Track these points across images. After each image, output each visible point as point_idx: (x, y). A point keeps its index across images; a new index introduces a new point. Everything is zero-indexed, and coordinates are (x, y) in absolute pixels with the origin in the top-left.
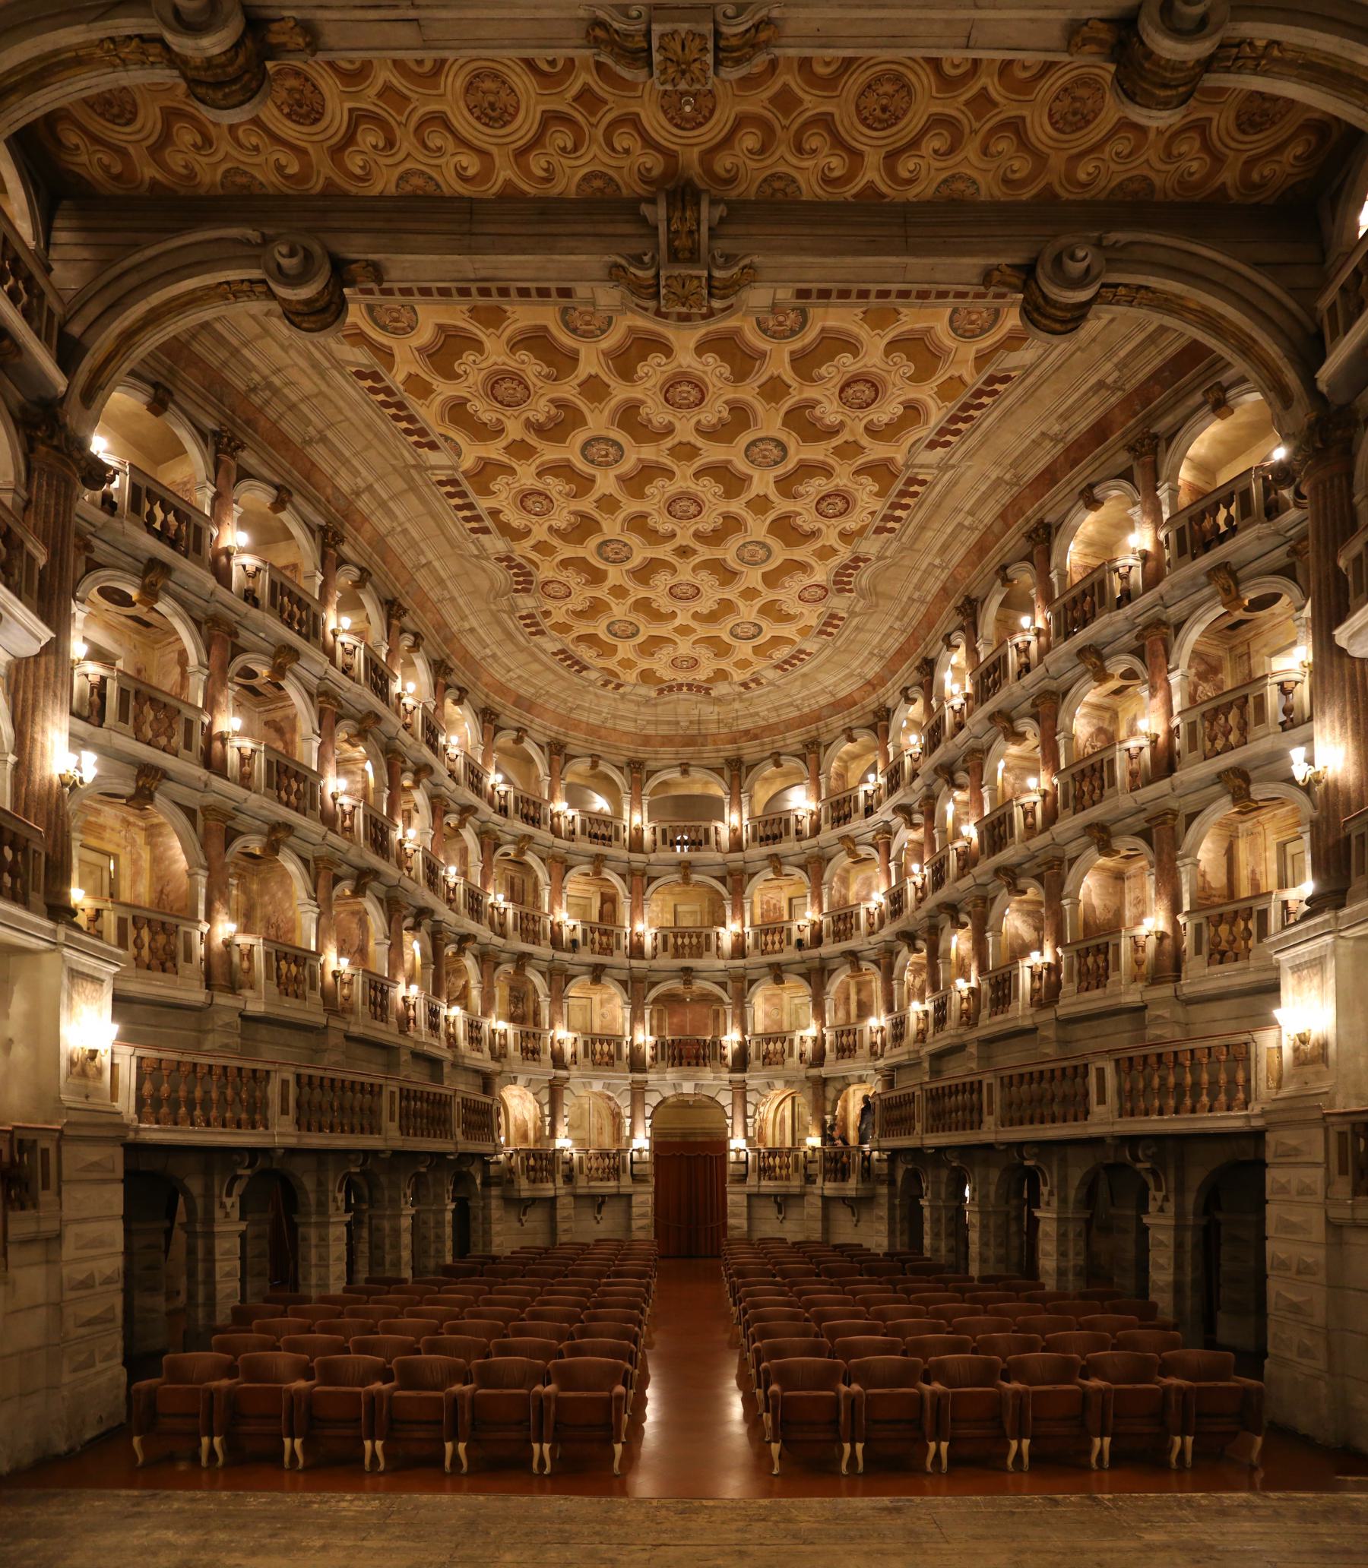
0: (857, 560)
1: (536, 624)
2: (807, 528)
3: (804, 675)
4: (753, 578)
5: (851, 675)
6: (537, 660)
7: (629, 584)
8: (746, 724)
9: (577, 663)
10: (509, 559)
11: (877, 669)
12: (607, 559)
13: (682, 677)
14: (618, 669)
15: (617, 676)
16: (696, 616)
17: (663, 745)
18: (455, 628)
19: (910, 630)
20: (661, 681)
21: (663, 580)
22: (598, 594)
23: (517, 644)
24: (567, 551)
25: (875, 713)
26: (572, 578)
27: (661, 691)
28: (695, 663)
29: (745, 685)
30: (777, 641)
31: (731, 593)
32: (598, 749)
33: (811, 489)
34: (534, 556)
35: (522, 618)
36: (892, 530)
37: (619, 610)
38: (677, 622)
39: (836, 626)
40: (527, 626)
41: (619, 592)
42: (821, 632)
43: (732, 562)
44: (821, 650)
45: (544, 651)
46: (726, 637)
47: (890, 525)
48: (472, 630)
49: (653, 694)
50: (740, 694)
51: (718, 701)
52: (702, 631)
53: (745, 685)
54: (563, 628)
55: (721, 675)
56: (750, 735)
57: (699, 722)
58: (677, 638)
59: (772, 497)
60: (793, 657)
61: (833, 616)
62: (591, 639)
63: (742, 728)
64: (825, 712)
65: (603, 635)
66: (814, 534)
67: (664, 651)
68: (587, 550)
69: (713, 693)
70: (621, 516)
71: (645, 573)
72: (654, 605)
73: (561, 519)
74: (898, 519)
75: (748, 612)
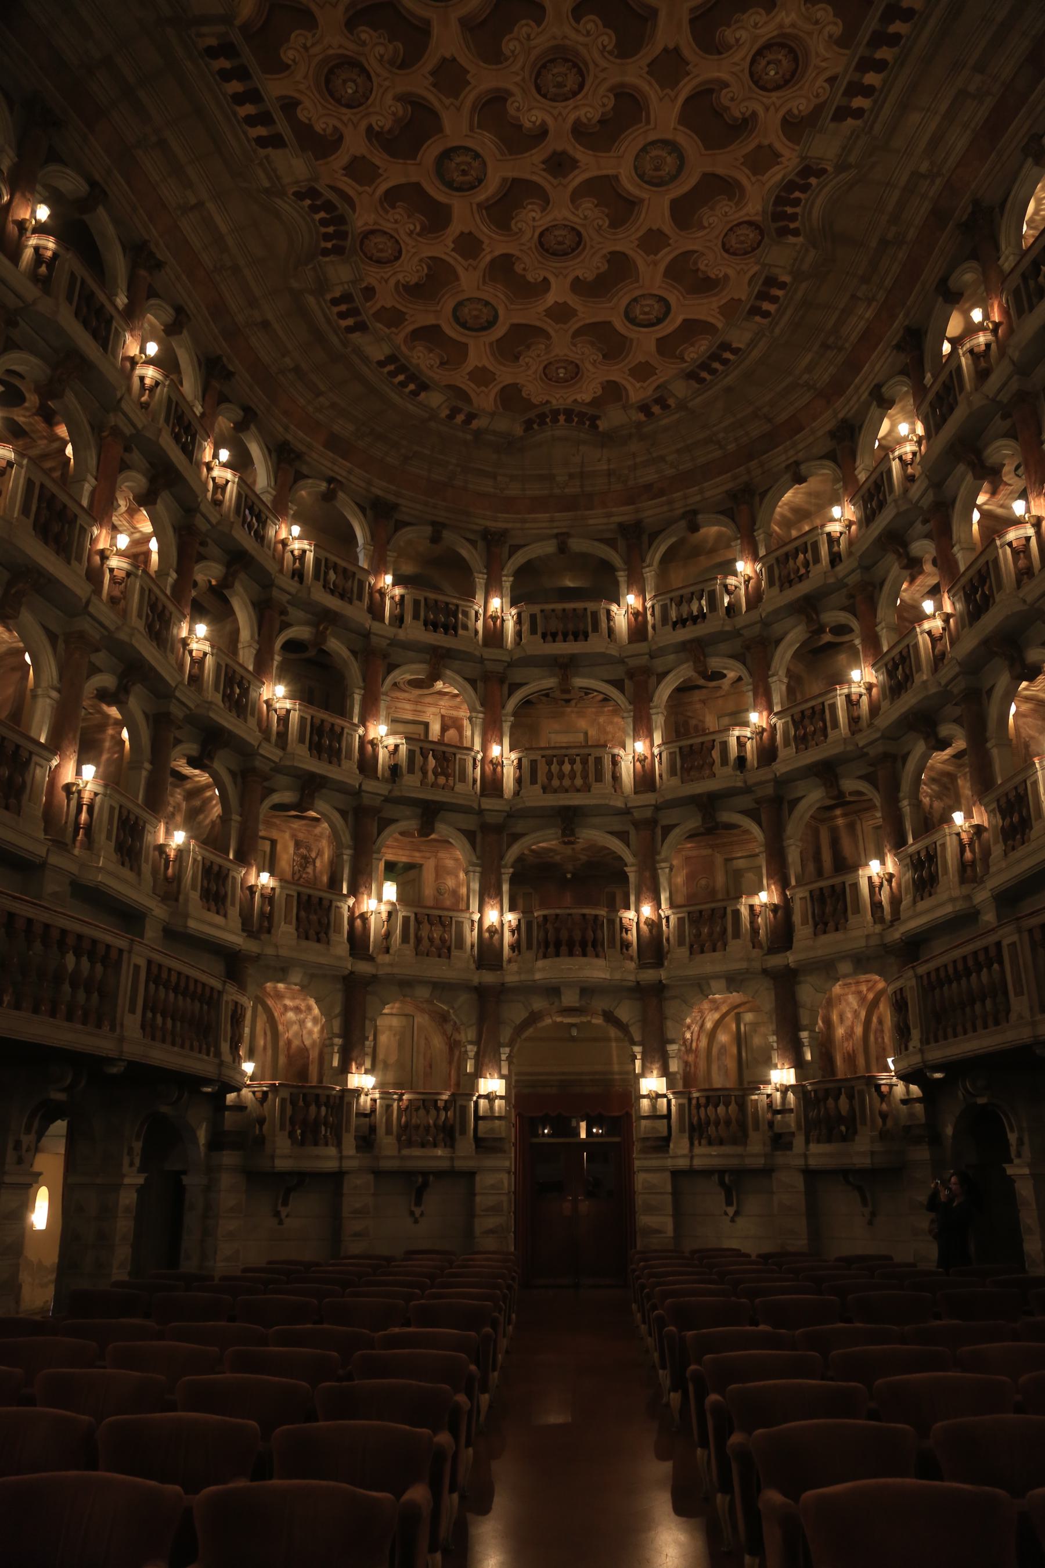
0: (807, 171)
1: (354, 312)
2: (737, 111)
4: (656, 210)
7: (485, 232)
9: (412, 378)
10: (312, 193)
12: (450, 185)
13: (560, 398)
14: (469, 387)
15: (465, 397)
16: (578, 286)
21: (531, 219)
22: (437, 251)
24: (395, 174)
25: (832, 434)
26: (401, 223)
27: (528, 425)
28: (575, 373)
30: (692, 328)
31: (626, 242)
33: (743, 35)
34: (347, 185)
35: (335, 302)
36: (859, 113)
37: (469, 281)
38: (551, 298)
39: (774, 300)
40: (342, 315)
41: (468, 246)
42: (755, 311)
43: (630, 185)
46: (620, 325)
47: (858, 102)
48: (265, 325)
49: (518, 430)
52: (587, 313)
53: (644, 408)
54: (394, 318)
55: (613, 391)
58: (550, 326)
59: (687, 53)
60: (714, 357)
61: (771, 281)
62: (430, 335)
65: (451, 331)
66: (745, 125)
68: (419, 171)
69: (602, 425)
70: (469, 97)
71: (502, 210)
72: (518, 268)
73: (385, 111)
74: (868, 91)
75: (651, 275)
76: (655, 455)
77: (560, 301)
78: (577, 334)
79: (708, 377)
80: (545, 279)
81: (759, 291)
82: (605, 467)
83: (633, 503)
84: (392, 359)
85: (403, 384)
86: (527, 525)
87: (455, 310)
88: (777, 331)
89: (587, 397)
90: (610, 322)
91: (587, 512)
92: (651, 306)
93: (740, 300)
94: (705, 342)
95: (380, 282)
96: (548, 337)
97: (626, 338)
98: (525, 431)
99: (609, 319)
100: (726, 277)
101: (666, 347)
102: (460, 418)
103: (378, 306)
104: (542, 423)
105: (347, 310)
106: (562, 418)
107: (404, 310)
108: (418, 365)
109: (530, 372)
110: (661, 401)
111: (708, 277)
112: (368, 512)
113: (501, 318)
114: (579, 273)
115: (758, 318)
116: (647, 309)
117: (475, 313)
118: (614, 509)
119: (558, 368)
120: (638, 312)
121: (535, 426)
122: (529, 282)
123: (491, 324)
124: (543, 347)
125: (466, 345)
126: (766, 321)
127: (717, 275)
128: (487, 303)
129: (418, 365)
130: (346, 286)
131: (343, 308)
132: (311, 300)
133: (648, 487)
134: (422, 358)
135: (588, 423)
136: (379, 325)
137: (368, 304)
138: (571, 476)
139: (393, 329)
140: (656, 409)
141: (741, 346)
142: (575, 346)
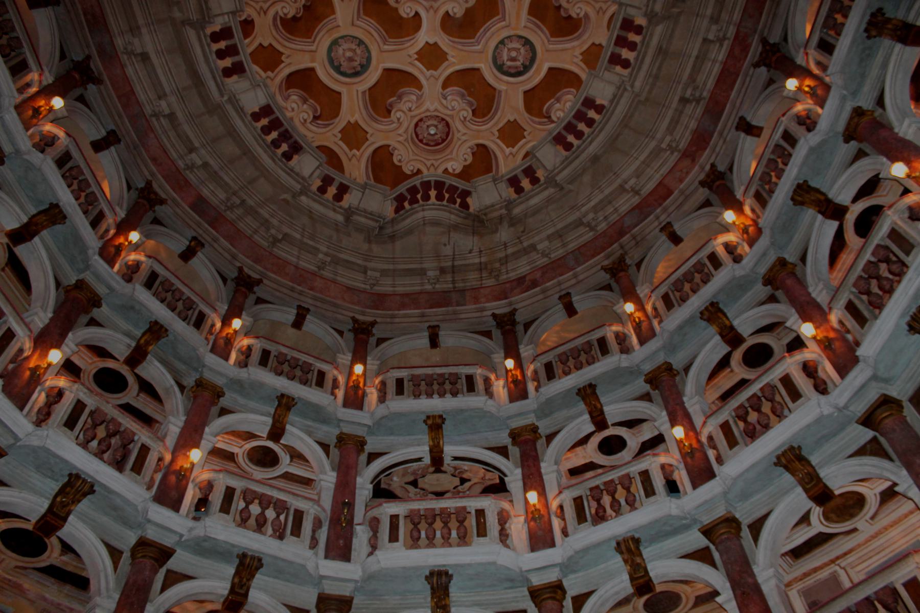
1: (232, 51)
3: (595, 159)
5: (656, 153)
6: (232, 133)
8: (521, 267)
9: (286, 136)
11: (693, 125)
14: (341, 149)
16: (448, 23)
17: (403, 306)
18: (119, 42)
19: (731, 32)
20: (399, 176)
23: (204, 97)
27: (400, 199)
29: (514, 182)
30: (559, 79)
32: (307, 302)
42: (615, 60)
44: (615, 99)
45: (240, 110)
48: (144, 57)
49: (389, 210)
50: (509, 205)
51: (479, 224)
55: (483, 159)
56: (523, 283)
57: (454, 270)
60: (580, 116)
61: (628, 25)
63: (513, 275)
64: (628, 222)
65: (325, 75)
67: (404, 105)
76: (525, 244)
77: (431, 42)
78: (445, 86)
79: (576, 142)
80: (417, 14)
81: (618, 37)
82: (477, 261)
83: (506, 298)
84: (266, 111)
85: (276, 144)
86: (397, 320)
87: (330, 50)
88: (638, 84)
89: (456, 166)
90: (478, 69)
91: (458, 308)
92: (517, 50)
93: (600, 45)
94: (570, 97)
95: (259, 14)
96: (420, 87)
97: (495, 89)
98: (397, 211)
99: (476, 66)
100: (586, 16)
101: (535, 101)
102: (332, 190)
103: (256, 44)
104: (414, 201)
105: (226, 47)
106: (433, 193)
107: (281, 49)
108: (292, 119)
109: (401, 131)
110: (529, 172)
111: (570, 17)
112: (229, 282)
113: (374, 61)
114: (448, 7)
115: (618, 69)
116: (514, 54)
117: (349, 54)
118: (487, 305)
119: (428, 127)
120: (505, 58)
121: (406, 204)
122: (401, 18)
123: (364, 67)
124: (414, 98)
125: (339, 94)
126: (626, 72)
127: (578, 15)
128: (361, 43)
129: (292, 119)
130: (226, 17)
131: (222, 45)
132: (191, 34)
133: (520, 280)
134: (296, 111)
135: (459, 200)
136: (256, 68)
137: (247, 41)
138: (443, 271)
139: (269, 73)
140: (525, 183)
141: (605, 103)
142: (446, 99)
